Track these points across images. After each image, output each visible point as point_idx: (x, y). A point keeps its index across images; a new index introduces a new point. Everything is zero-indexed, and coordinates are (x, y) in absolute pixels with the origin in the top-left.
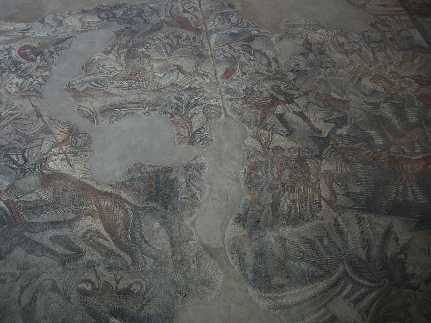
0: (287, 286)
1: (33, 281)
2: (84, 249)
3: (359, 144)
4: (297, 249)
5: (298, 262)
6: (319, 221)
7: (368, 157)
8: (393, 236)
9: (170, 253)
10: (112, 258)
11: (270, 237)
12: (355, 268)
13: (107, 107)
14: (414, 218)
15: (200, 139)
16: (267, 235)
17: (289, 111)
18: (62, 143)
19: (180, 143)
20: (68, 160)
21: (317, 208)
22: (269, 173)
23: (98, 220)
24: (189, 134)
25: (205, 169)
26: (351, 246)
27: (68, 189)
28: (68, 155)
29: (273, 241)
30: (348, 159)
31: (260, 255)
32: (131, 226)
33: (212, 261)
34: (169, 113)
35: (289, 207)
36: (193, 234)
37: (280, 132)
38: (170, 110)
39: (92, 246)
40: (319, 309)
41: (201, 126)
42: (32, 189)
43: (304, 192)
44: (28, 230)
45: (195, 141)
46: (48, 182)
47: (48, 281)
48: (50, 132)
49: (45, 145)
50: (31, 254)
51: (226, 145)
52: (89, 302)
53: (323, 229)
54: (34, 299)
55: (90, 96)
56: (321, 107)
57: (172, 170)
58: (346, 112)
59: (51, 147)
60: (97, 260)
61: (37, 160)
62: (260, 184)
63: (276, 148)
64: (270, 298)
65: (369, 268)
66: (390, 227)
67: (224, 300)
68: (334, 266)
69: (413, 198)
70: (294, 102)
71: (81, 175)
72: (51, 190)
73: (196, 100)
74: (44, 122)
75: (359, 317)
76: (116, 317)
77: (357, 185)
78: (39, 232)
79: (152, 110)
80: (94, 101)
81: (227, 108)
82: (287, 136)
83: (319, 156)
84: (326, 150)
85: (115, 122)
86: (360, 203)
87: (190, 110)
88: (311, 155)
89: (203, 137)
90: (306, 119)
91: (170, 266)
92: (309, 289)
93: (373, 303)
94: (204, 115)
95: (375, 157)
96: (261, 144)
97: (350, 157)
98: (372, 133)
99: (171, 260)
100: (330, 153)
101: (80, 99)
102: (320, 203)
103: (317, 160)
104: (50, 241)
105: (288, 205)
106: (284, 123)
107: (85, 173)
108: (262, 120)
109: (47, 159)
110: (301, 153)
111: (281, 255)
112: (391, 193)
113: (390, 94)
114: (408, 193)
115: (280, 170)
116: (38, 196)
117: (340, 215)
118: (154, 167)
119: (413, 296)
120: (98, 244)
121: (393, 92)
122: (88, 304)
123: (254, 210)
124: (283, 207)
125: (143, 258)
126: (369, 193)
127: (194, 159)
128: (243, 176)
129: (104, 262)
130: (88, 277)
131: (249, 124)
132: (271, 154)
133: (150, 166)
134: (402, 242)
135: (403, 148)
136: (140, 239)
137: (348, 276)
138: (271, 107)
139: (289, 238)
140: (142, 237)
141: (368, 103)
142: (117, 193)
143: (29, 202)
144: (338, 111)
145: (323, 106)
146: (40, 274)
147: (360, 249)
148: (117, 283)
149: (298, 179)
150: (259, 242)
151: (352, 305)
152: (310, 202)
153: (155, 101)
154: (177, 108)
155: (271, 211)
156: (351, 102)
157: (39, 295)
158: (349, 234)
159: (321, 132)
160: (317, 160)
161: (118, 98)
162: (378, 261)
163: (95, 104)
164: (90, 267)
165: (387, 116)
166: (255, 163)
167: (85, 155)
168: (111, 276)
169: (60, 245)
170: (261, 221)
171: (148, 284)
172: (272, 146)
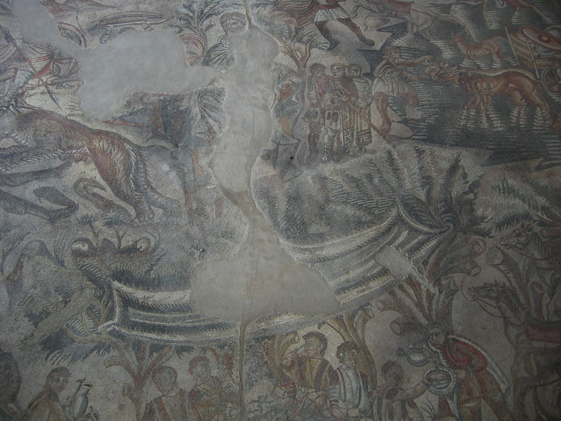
0: (328, 235)
1: (16, 244)
2: (76, 202)
3: (422, 58)
4: (340, 190)
5: (342, 206)
7: (433, 74)
9: (183, 201)
10: (111, 211)
11: (307, 177)
12: (412, 212)
13: (96, 23)
14: (488, 149)
15: (217, 58)
16: (303, 174)
17: (333, 18)
18: (41, 72)
19: (191, 64)
20: (50, 93)
21: (366, 139)
22: (306, 98)
23: (93, 166)
24: (203, 52)
25: (225, 96)
26: (408, 185)
27: (52, 130)
28: (50, 87)
29: (311, 181)
30: (406, 78)
31: (294, 199)
32: (133, 171)
33: (235, 208)
34: (177, 26)
35: (331, 139)
36: (211, 177)
37: (321, 46)
38: (179, 23)
39: (87, 198)
40: (366, 261)
41: (219, 42)
42: (7, 132)
43: (350, 120)
44: (6, 184)
45: (211, 61)
46: (26, 122)
47: (34, 243)
48: (25, 59)
49: (20, 76)
50: (12, 212)
51: (251, 64)
52: (86, 265)
53: (373, 165)
54: (19, 266)
55: (74, 9)
57: (183, 99)
58: (407, 17)
59: (27, 78)
60: (94, 214)
61: (11, 96)
62: (294, 111)
63: (315, 66)
64: (306, 250)
65: (429, 211)
66: (457, 161)
67: (251, 254)
68: (386, 210)
69: (487, 124)
70: (339, 6)
71: (68, 112)
72: (31, 132)
73: (212, 8)
74: (16, 47)
75: (415, 270)
76: (120, 281)
77: (418, 110)
78: (19, 185)
79: (155, 24)
80: (79, 16)
81: (252, 17)
82: (329, 49)
83: (369, 74)
85: (108, 42)
86: (420, 132)
87: (204, 21)
88: (360, 74)
89: (221, 56)
90: (354, 27)
91: (183, 216)
92: (355, 238)
93: (433, 252)
94: (223, 27)
95: (442, 75)
96: (296, 60)
97: (409, 75)
98: (440, 44)
99: (184, 209)
100: (384, 71)
101: (61, 14)
102: (370, 133)
103: (367, 79)
104: (33, 195)
105: (329, 136)
106: (325, 34)
107: (73, 108)
108: (297, 30)
109: (23, 93)
110: (346, 71)
111: (320, 198)
112: (460, 118)
114: (482, 119)
115: (319, 94)
116: (16, 141)
117: (394, 147)
118: (160, 95)
119: (482, 244)
120: (94, 195)
122: (85, 267)
123: (287, 144)
124: (323, 139)
125: (150, 209)
127: (210, 84)
128: (272, 102)
129: (102, 216)
130: (84, 236)
131: (280, 36)
132: (308, 73)
133: (154, 95)
134: (471, 178)
135: (478, 62)
136: (146, 186)
137: (403, 221)
138: (309, 13)
139: (330, 177)
140: (148, 183)
142: (114, 131)
143: (4, 149)
144: (396, 16)
145: (376, 10)
146: (24, 236)
148: (120, 240)
150: (293, 183)
151: (407, 255)
152: (358, 132)
153: (158, 12)
154: (187, 19)
155: (307, 144)
156: (413, 5)
157: (25, 260)
158: (405, 171)
159: (373, 44)
160: (367, 79)
161: (109, 10)
162: (441, 202)
163: (80, 20)
164: (85, 224)
165: (460, 22)
166: (288, 86)
167: (72, 86)
168: (111, 232)
169: (47, 199)
170: (295, 158)
171: (157, 239)
172: (309, 63)
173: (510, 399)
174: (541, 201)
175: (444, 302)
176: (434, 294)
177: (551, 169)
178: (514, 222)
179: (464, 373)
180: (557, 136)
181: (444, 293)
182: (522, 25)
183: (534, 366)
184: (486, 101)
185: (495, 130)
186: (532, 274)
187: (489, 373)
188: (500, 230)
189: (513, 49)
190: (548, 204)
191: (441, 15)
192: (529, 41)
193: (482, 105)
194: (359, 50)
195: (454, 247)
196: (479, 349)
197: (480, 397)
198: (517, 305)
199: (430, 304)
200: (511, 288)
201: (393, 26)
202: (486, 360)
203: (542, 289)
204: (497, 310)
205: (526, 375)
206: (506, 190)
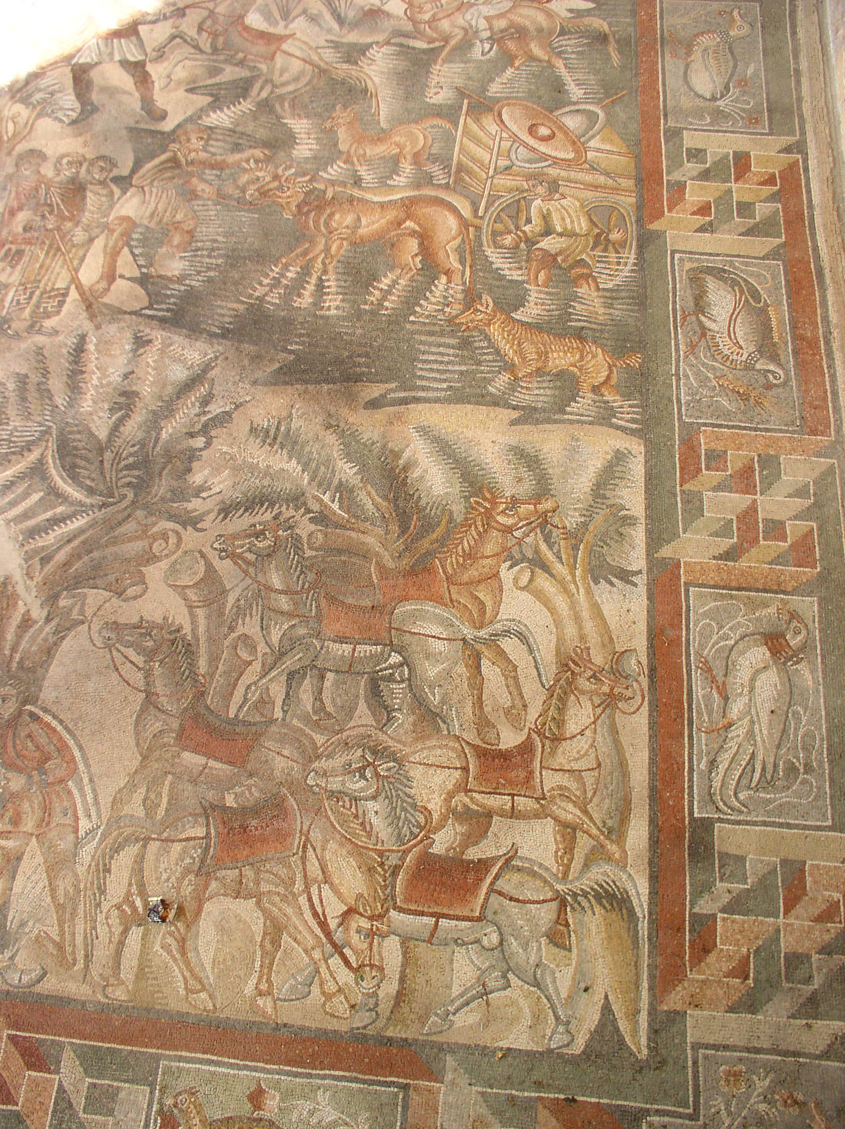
6: (40, 339)
8: (203, 390)
26: (86, 405)
37: (60, 115)
43: (41, 267)
53: (41, 357)
56: (201, 51)
65: (102, 461)
69: (310, 300)
84: (149, 166)
86: (162, 303)
93: (69, 541)
97: (201, 186)
98: (299, 126)
102: (65, 295)
110: (84, 168)
112: (261, 284)
113: (415, 22)
114: (304, 288)
117: (98, 327)
119: (173, 540)
121: (427, 17)
126: (201, 278)
134: (215, 409)
135: (363, 171)
141: (336, 45)
144: (241, 63)
147: (101, 414)
149: (44, 232)
156: (289, 41)
159: (163, 116)
162: (134, 446)
173: (86, 854)
174: (347, 471)
175: (45, 640)
176: (36, 622)
177: (402, 408)
178: (262, 505)
179: (23, 781)
180: (453, 341)
181: (53, 623)
182: (508, 98)
183: (165, 800)
184: (333, 250)
185: (323, 313)
186: (248, 619)
187: (69, 792)
188: (225, 518)
189: (457, 149)
190: (356, 481)
191: (338, 66)
192: (504, 135)
193: (320, 260)
194: (131, 130)
195: (115, 537)
196: (71, 743)
197: (32, 835)
198: (187, 673)
199: (19, 637)
200: (189, 638)
201: (224, 83)
202: (76, 768)
203: (253, 649)
204: (140, 675)
205: (141, 813)
206: (278, 441)
